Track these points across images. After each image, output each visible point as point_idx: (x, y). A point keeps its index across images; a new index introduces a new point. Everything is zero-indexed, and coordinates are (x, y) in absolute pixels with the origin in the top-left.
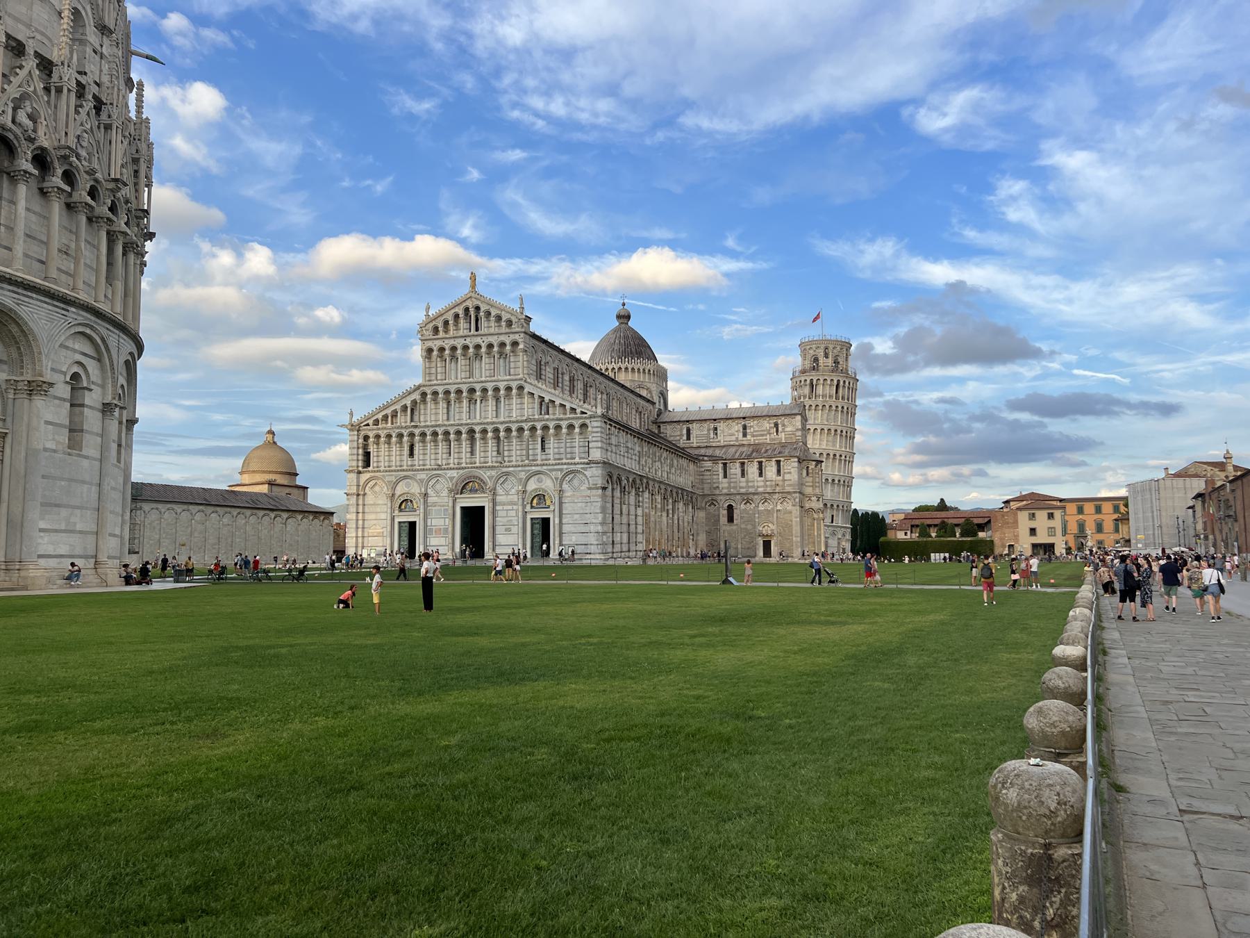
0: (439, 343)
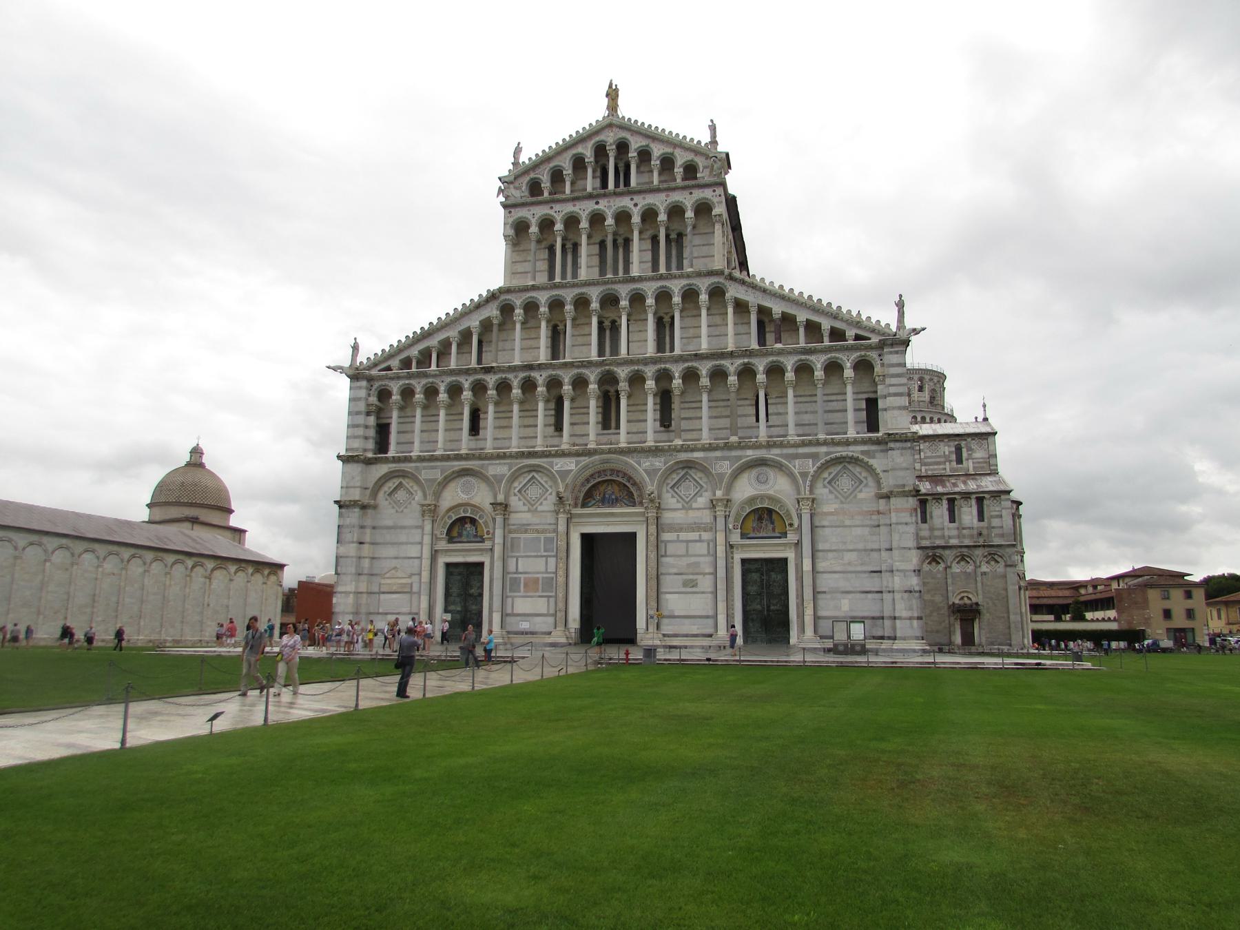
0: (541, 211)
